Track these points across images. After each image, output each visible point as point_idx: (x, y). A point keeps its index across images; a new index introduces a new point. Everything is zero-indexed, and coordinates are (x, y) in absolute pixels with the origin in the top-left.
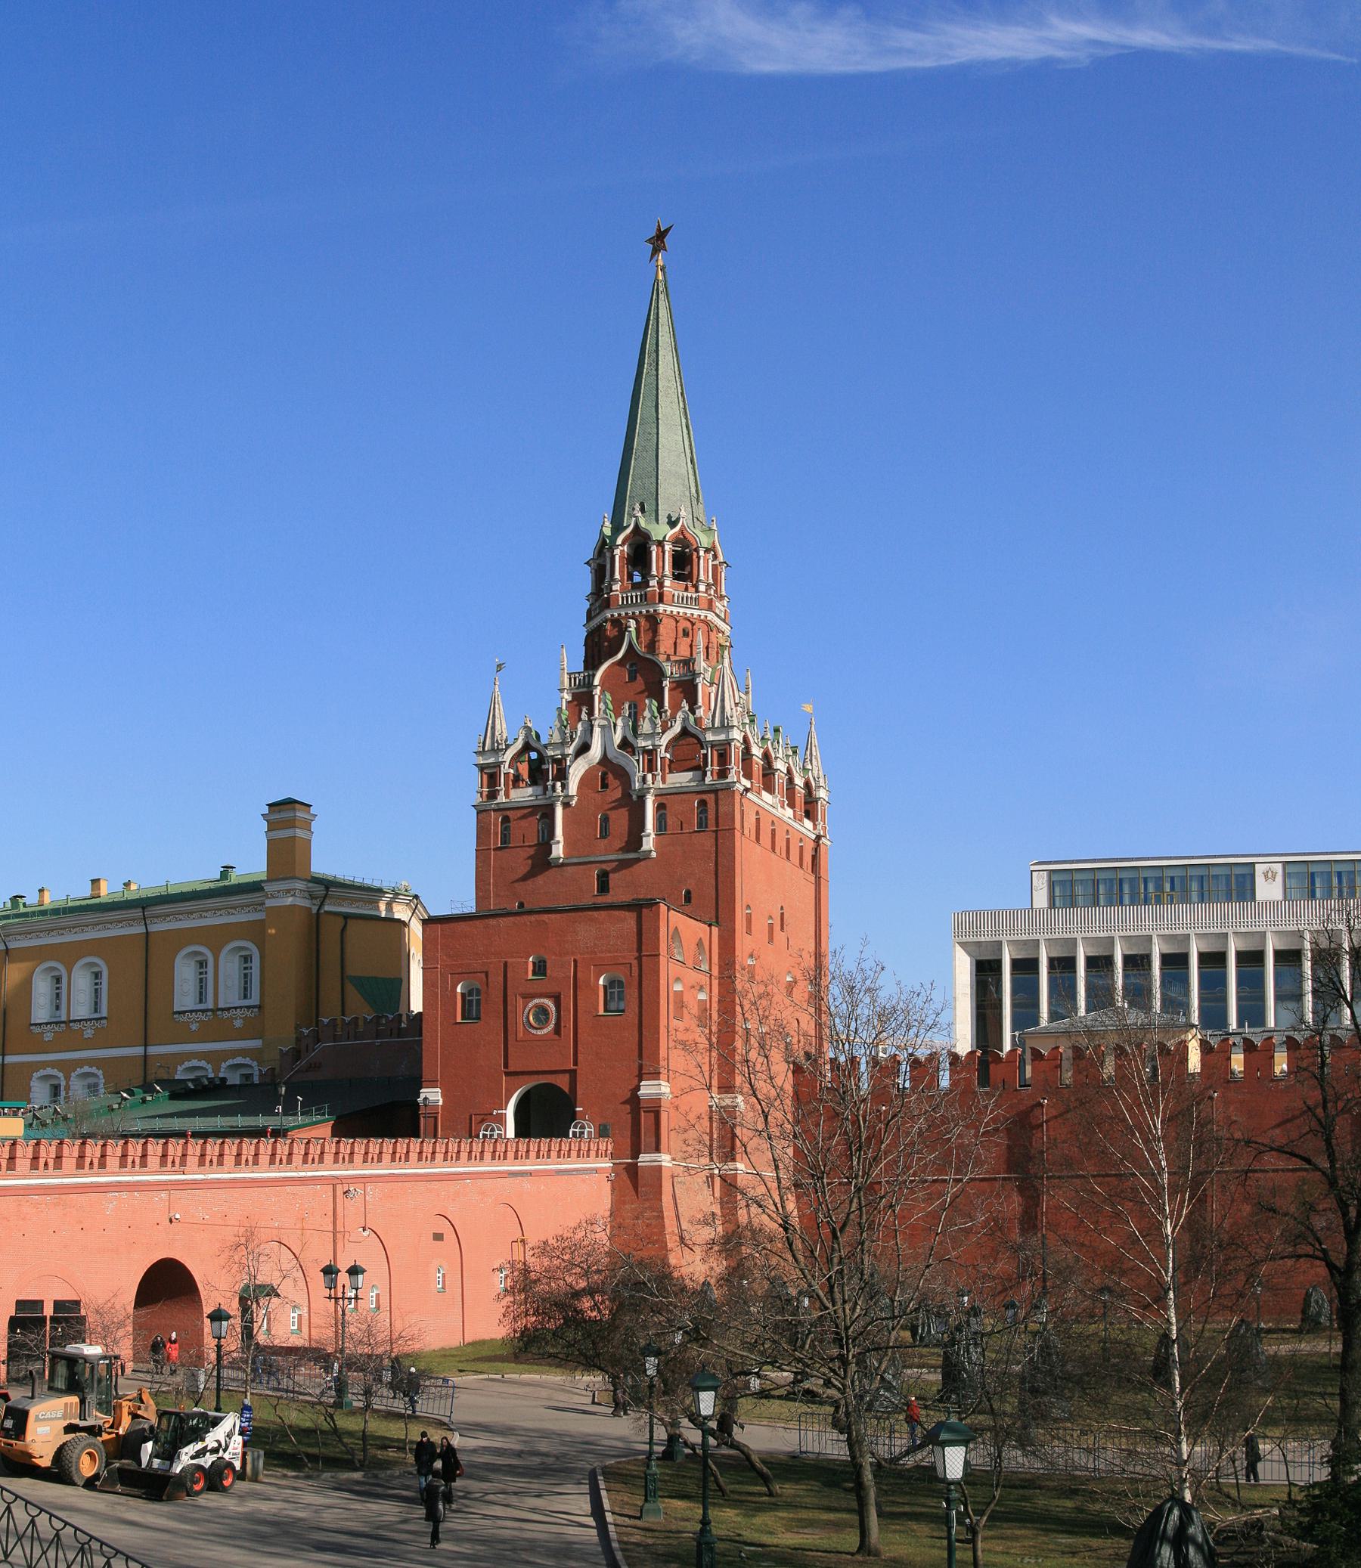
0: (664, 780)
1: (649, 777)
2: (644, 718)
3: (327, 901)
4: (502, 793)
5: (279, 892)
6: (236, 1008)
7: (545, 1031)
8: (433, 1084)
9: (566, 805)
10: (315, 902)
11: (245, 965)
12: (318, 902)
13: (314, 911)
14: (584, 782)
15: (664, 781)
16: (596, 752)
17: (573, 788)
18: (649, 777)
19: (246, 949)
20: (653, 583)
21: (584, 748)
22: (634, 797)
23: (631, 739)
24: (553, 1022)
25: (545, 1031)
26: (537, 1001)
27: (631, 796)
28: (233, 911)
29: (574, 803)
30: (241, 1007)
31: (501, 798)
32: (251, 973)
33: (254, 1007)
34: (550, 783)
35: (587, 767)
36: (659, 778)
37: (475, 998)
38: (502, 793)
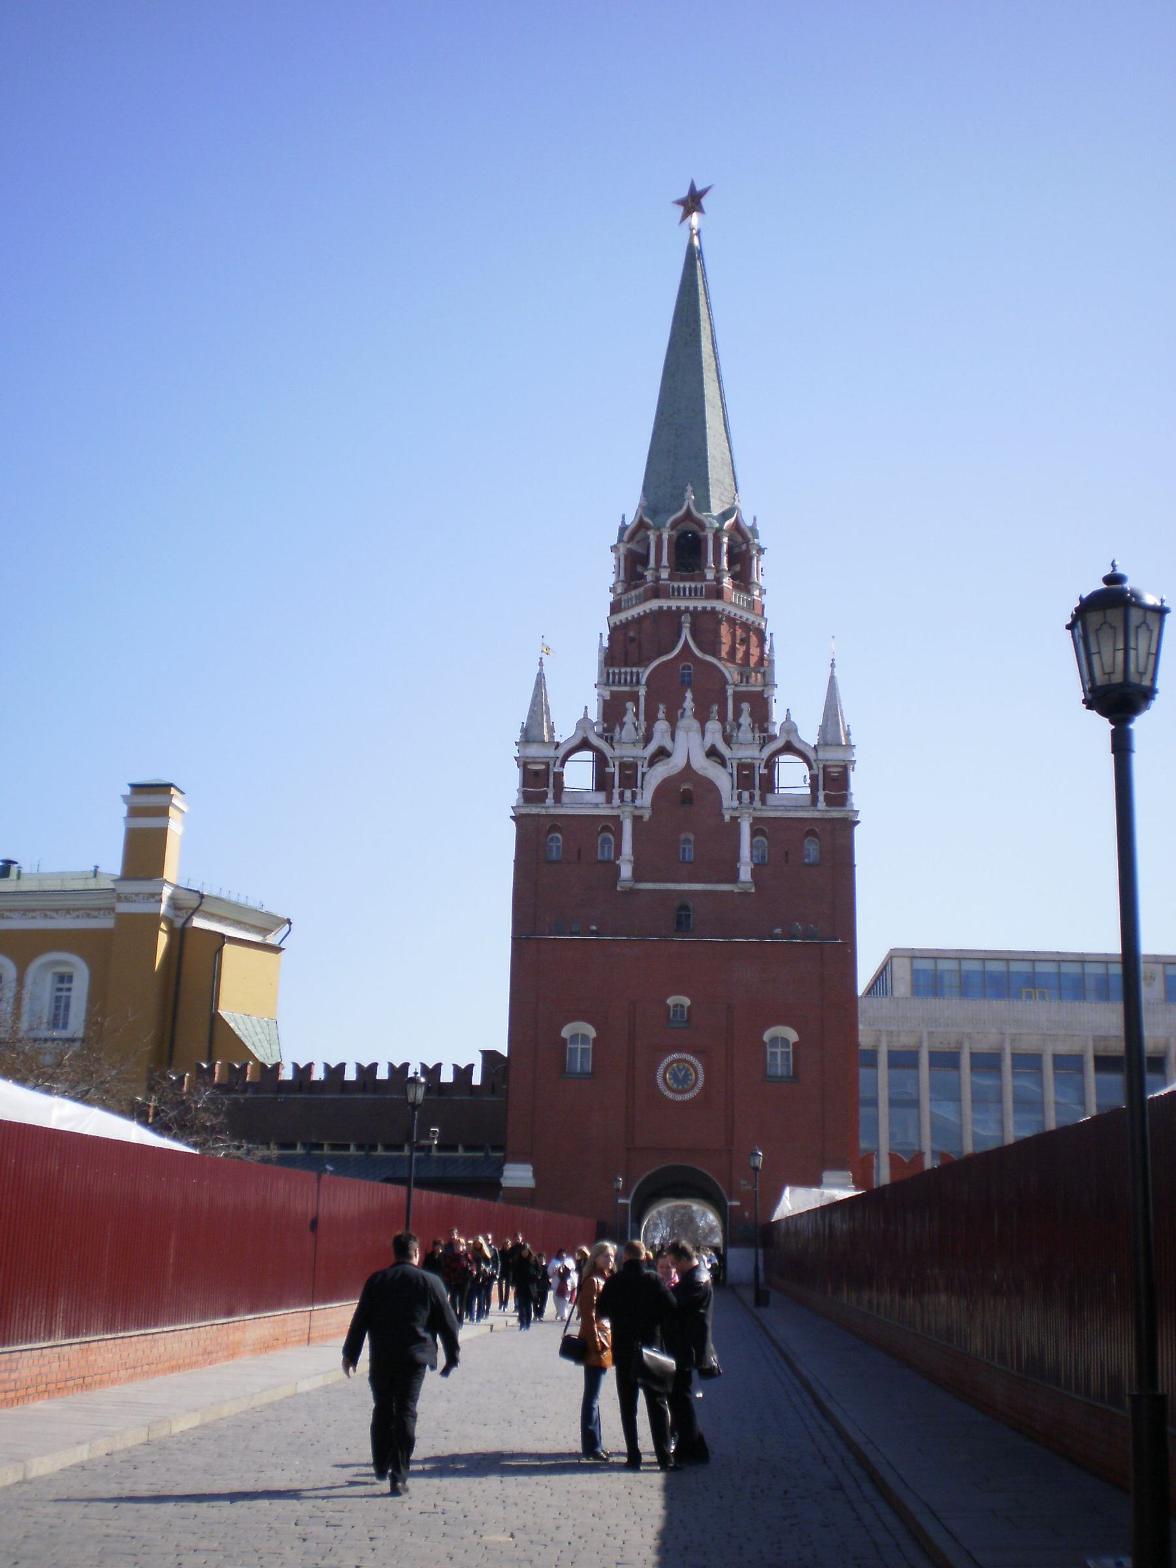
0: (763, 801)
1: (746, 795)
3: (196, 914)
4: (550, 795)
5: (137, 895)
6: (46, 1040)
8: (520, 1158)
9: (637, 819)
10: (178, 913)
11: (60, 986)
12: (184, 915)
13: (179, 923)
15: (763, 801)
16: (676, 763)
18: (746, 795)
19: (66, 963)
20: (710, 575)
21: (662, 754)
22: (727, 818)
23: (722, 747)
26: (676, 1056)
27: (722, 816)
28: (53, 914)
29: (647, 815)
30: (54, 1040)
31: (550, 801)
32: (68, 998)
33: (73, 1040)
34: (616, 792)
35: (665, 775)
36: (757, 798)
37: (580, 1046)
38: (550, 795)
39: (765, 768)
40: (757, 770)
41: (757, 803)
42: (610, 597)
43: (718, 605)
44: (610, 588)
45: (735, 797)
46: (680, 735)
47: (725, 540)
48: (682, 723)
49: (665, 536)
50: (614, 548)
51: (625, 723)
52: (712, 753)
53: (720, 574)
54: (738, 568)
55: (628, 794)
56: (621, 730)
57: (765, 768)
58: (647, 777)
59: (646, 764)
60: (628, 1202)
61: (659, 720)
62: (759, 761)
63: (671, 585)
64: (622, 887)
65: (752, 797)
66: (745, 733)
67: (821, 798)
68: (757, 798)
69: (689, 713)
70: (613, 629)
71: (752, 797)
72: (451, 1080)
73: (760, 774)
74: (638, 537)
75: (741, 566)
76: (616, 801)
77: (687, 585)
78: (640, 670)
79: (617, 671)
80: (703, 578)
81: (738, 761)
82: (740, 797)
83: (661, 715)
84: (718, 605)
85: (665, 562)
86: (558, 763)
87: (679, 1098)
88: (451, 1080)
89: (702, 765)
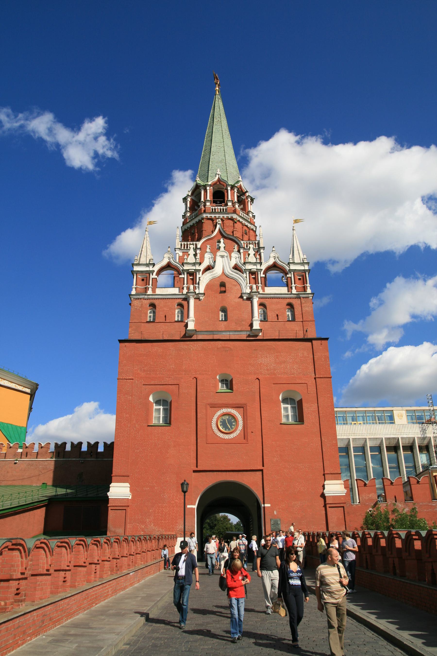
0: (264, 291)
1: (254, 286)
2: (249, 255)
4: (150, 289)
7: (232, 436)
14: (208, 287)
16: (218, 271)
17: (202, 290)
18: (254, 286)
20: (230, 204)
21: (209, 268)
24: (240, 427)
25: (232, 436)
26: (225, 410)
36: (260, 288)
38: (150, 289)
39: (263, 274)
40: (259, 275)
41: (260, 291)
42: (183, 220)
43: (235, 216)
44: (183, 215)
45: (248, 288)
46: (218, 259)
47: (236, 190)
48: (219, 254)
49: (208, 188)
50: (185, 199)
51: (189, 254)
52: (236, 268)
53: (234, 204)
54: (242, 206)
55: (192, 287)
56: (188, 257)
57: (263, 274)
58: (201, 279)
59: (201, 273)
60: (195, 507)
61: (207, 252)
62: (260, 270)
63: (211, 208)
64: (188, 334)
65: (257, 288)
66: (252, 259)
67: (294, 288)
68: (260, 288)
69: (222, 249)
70: (184, 231)
71: (257, 288)
72: (102, 450)
73: (261, 277)
74: (195, 194)
75: (243, 206)
76: (185, 291)
77: (219, 208)
78: (197, 243)
79: (186, 243)
80: (226, 205)
81: (249, 271)
82: (251, 288)
83: (208, 250)
84: (235, 216)
85: (208, 198)
86: (155, 274)
87: (226, 437)
88: (102, 450)
89: (229, 271)
